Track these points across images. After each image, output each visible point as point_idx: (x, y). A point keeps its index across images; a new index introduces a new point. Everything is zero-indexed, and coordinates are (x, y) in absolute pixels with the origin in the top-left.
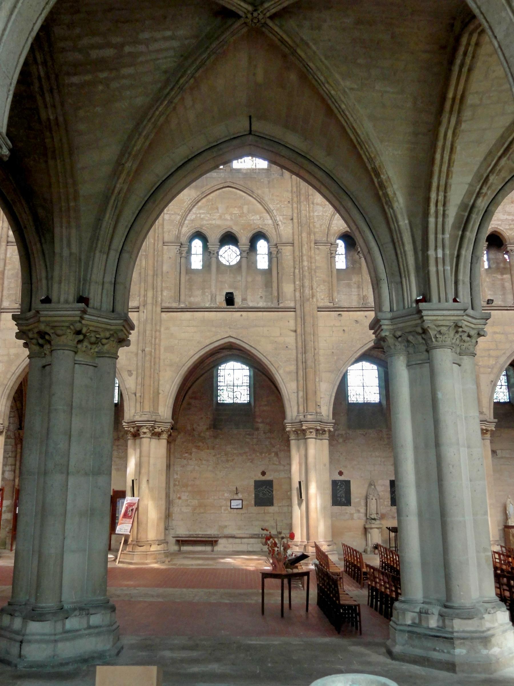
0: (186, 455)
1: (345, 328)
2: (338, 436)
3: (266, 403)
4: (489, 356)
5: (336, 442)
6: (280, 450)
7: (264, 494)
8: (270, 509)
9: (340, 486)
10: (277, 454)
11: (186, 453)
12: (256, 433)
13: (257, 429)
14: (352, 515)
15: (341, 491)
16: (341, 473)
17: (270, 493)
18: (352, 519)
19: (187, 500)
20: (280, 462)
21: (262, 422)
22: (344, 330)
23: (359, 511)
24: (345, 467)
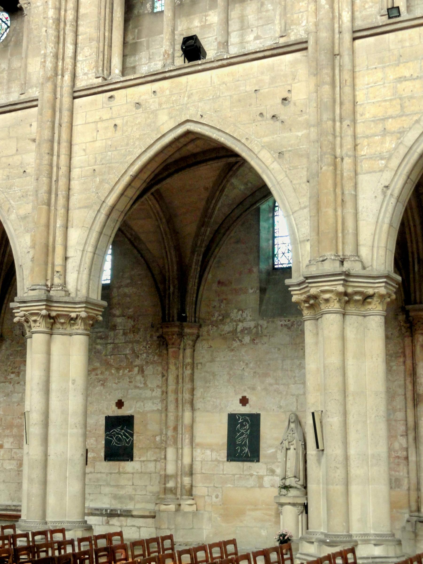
0: (12, 376)
1: (118, 122)
2: (242, 331)
3: (129, 281)
4: (385, 132)
5: (239, 343)
6: (147, 362)
7: (119, 440)
8: (128, 466)
9: (242, 425)
10: (142, 371)
11: (13, 373)
12: (112, 334)
13: (114, 328)
14: (260, 478)
15: (243, 434)
16: (244, 401)
17: (127, 438)
18: (261, 486)
19: (11, 449)
20: (145, 384)
21: (122, 315)
22: (115, 125)
23: (273, 472)
24: (253, 389)
